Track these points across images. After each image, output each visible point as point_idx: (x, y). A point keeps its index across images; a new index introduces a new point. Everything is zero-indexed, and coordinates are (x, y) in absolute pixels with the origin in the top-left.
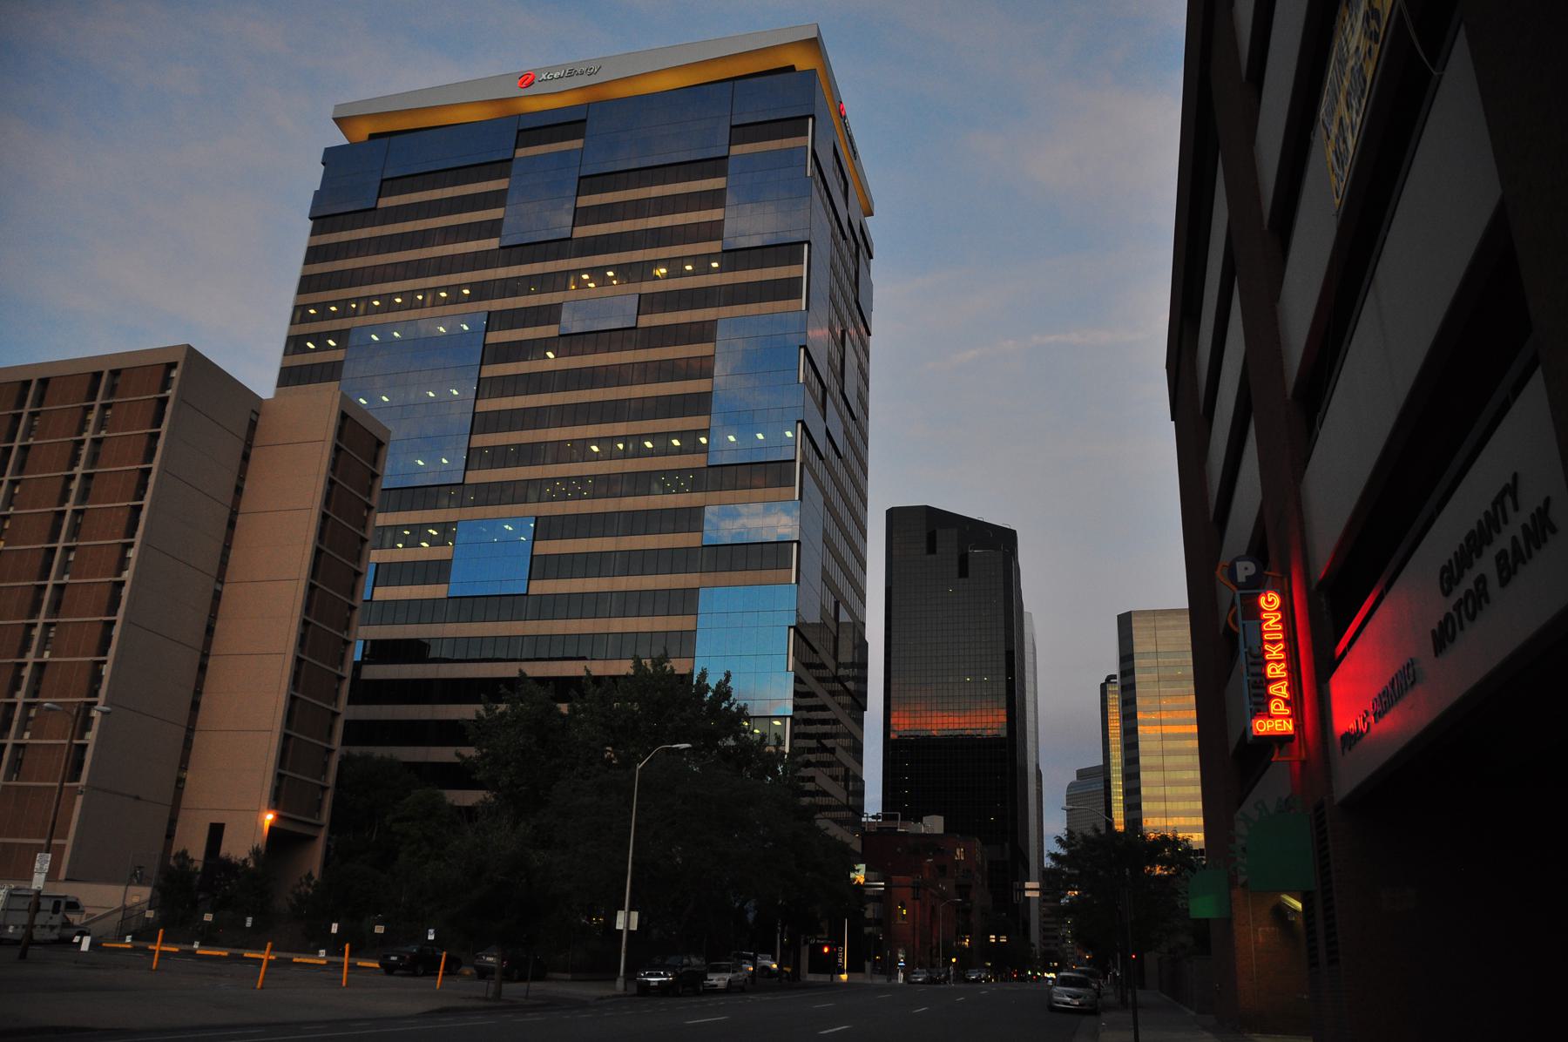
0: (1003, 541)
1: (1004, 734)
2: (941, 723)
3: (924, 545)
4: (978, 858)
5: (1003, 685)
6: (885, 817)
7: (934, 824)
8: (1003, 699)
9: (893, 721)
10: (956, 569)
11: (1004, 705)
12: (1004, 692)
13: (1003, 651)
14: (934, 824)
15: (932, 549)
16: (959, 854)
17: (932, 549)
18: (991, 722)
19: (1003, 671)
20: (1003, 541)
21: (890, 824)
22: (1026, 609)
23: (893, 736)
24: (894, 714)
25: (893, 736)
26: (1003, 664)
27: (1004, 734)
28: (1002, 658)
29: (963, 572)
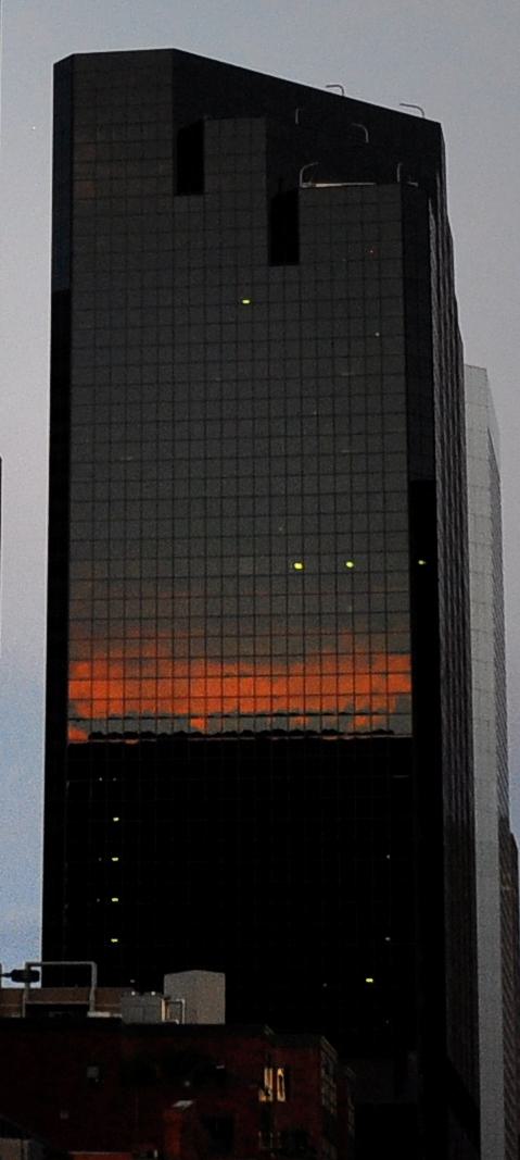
0: (397, 158)
1: (404, 727)
2: (218, 695)
3: (166, 168)
4: (328, 1095)
5: (401, 584)
6: (51, 976)
7: (197, 997)
8: (402, 625)
9: (74, 689)
10: (262, 238)
11: (405, 640)
12: (404, 602)
13: (401, 482)
14: (197, 997)
15: (189, 178)
16: (272, 1085)
17: (189, 178)
18: (362, 692)
19: (402, 542)
20: (397, 158)
21: (66, 996)
22: (469, 357)
23: (76, 734)
24: (78, 669)
25: (76, 734)
26: (402, 520)
27: (404, 727)
28: (400, 503)
29: (284, 248)
